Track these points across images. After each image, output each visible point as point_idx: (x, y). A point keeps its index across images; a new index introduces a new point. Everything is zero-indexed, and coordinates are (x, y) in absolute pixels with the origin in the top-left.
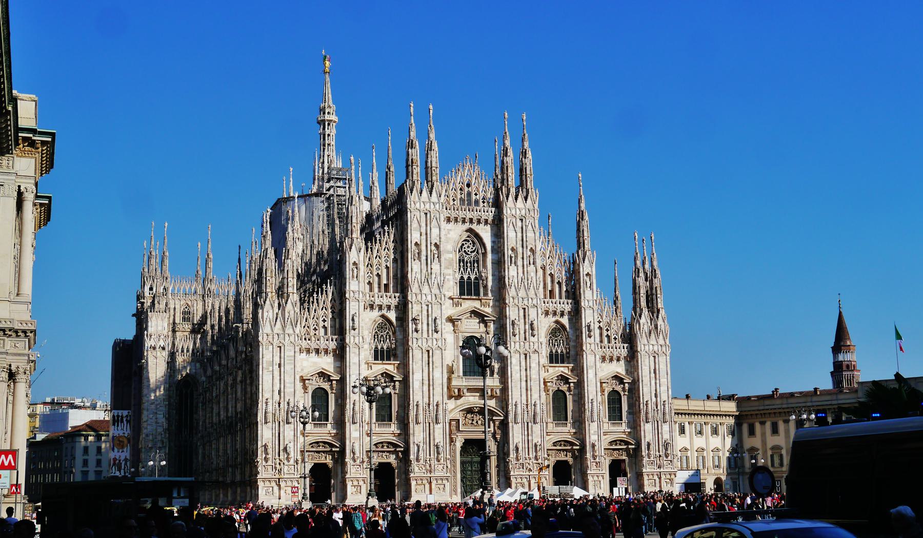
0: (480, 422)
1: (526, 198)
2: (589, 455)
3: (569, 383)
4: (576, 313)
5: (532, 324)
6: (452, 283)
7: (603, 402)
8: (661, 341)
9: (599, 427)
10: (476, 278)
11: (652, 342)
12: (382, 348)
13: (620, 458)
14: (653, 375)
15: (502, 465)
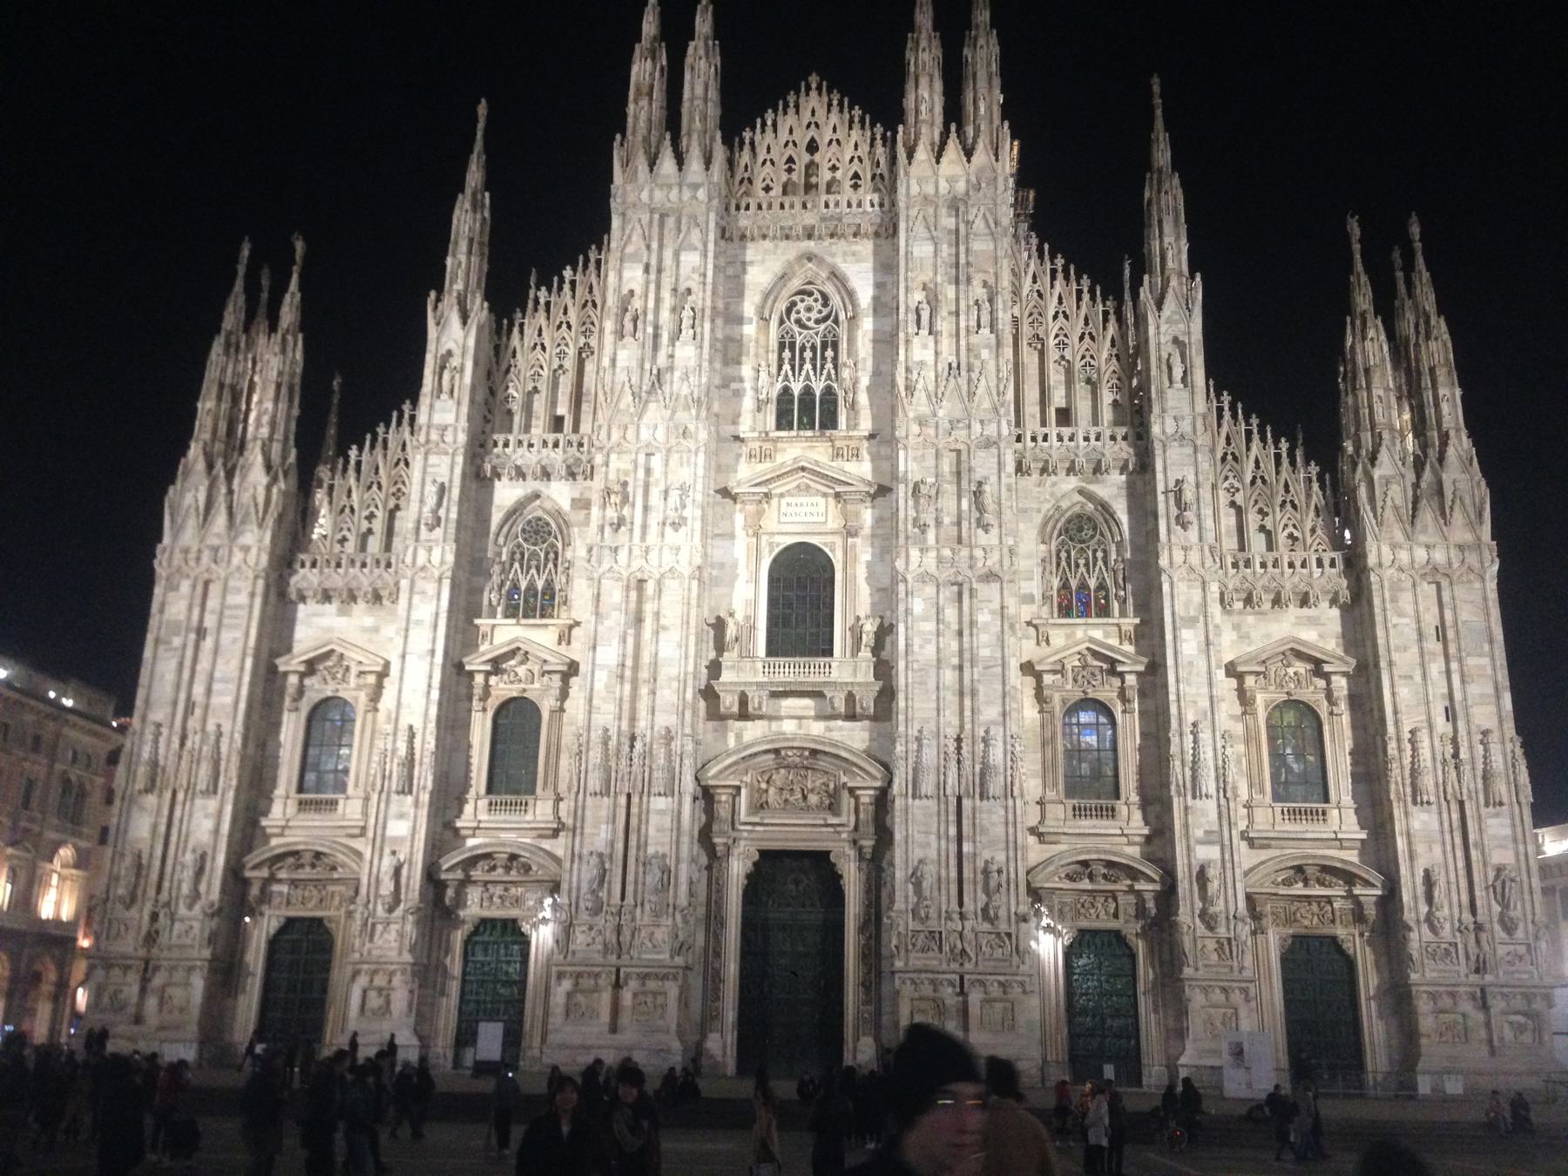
0: (813, 799)
1: (969, 153)
2: (1186, 915)
3: (1121, 675)
4: (1142, 467)
5: (978, 494)
6: (748, 403)
7: (1250, 739)
8: (1460, 532)
9: (1224, 815)
10: (828, 391)
11: (1423, 538)
12: (531, 587)
13: (1327, 930)
14: (1433, 645)
15: (884, 935)
